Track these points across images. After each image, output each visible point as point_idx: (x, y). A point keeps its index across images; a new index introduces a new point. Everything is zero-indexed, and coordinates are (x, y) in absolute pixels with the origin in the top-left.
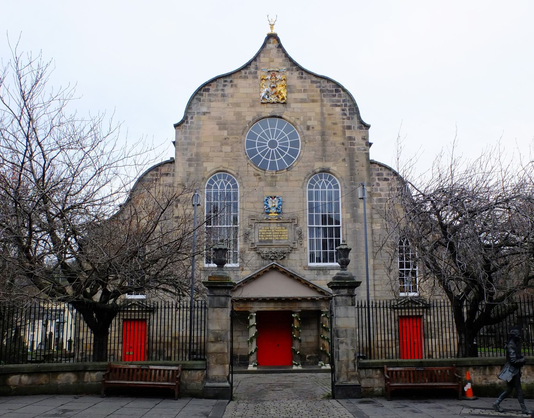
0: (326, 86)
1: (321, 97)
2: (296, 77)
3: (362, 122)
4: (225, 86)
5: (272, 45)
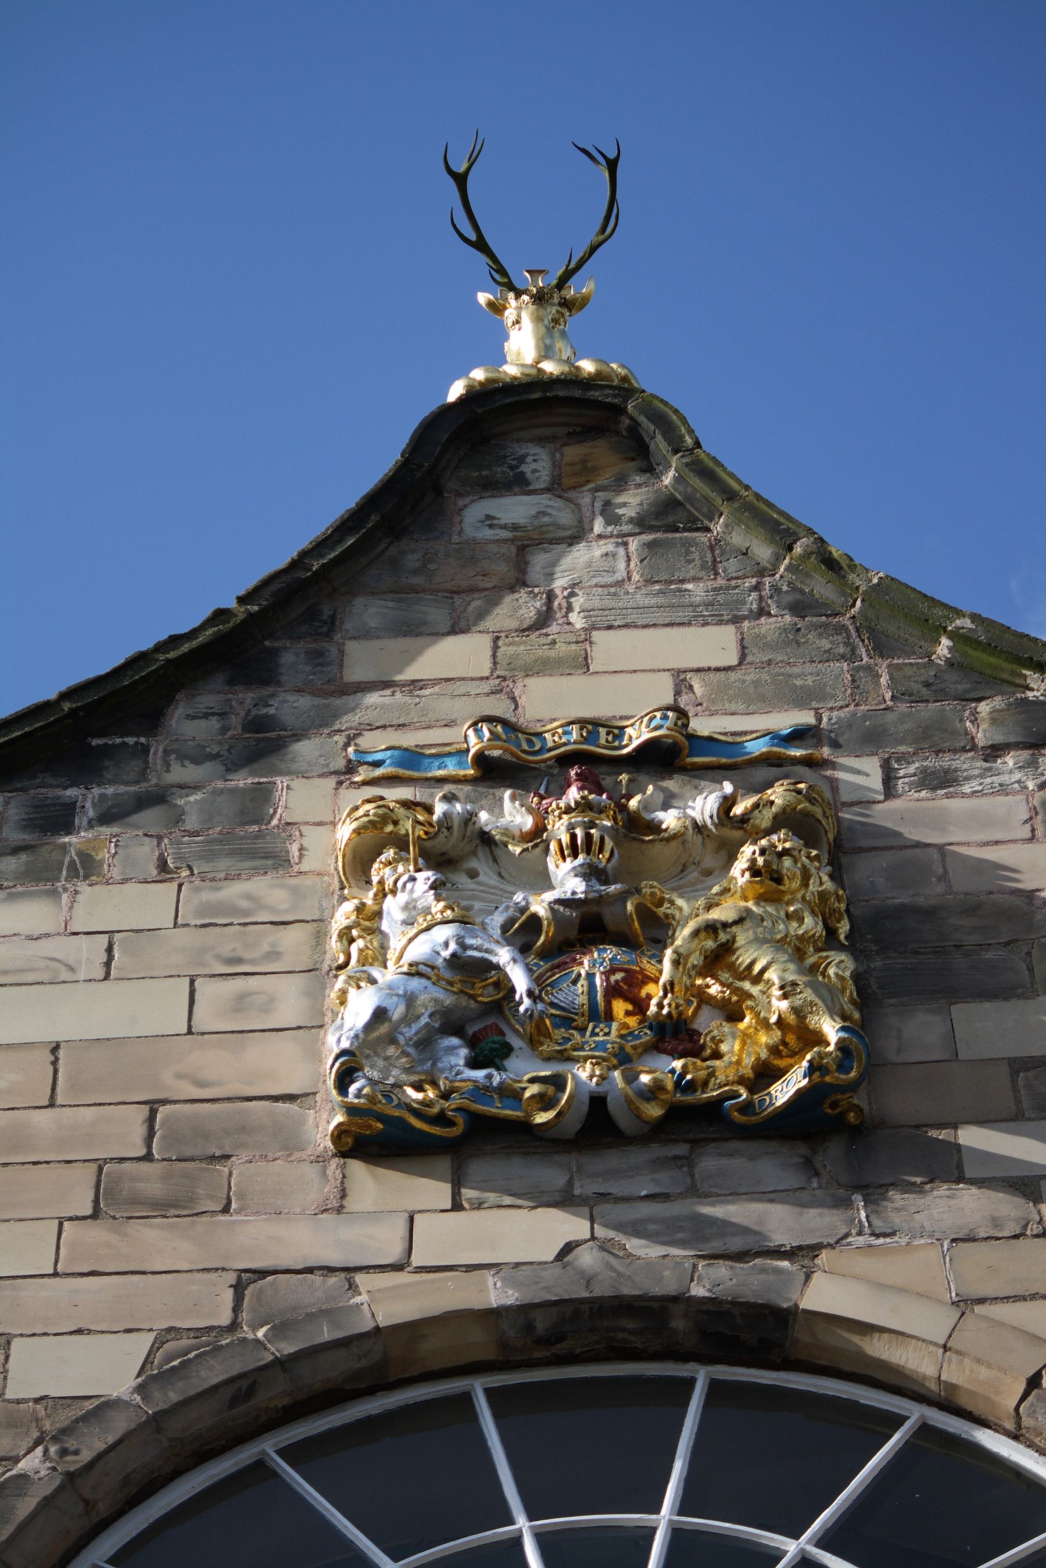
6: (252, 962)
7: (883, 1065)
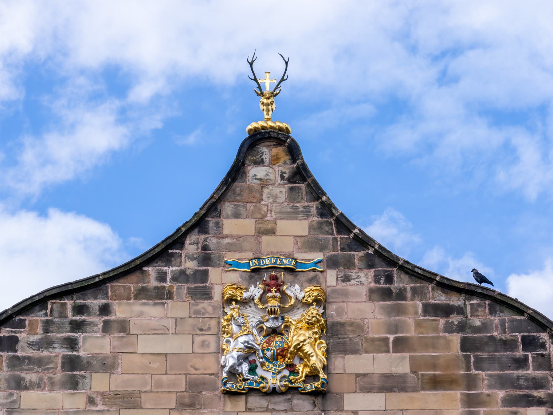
0: (484, 327)
1: (469, 369)
2: (363, 291)
4: (77, 326)
6: (205, 331)
7: (330, 374)
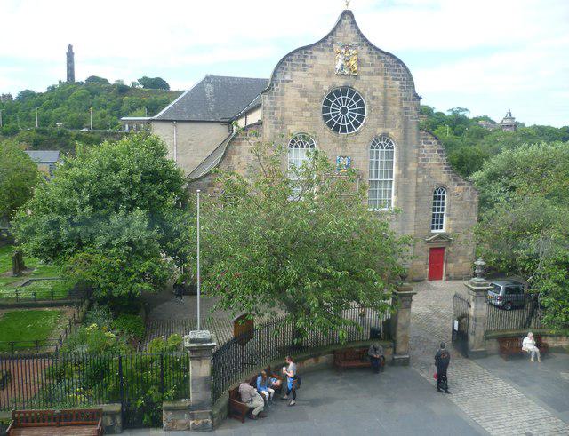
3: (416, 95)
4: (305, 57)
5: (346, 21)
